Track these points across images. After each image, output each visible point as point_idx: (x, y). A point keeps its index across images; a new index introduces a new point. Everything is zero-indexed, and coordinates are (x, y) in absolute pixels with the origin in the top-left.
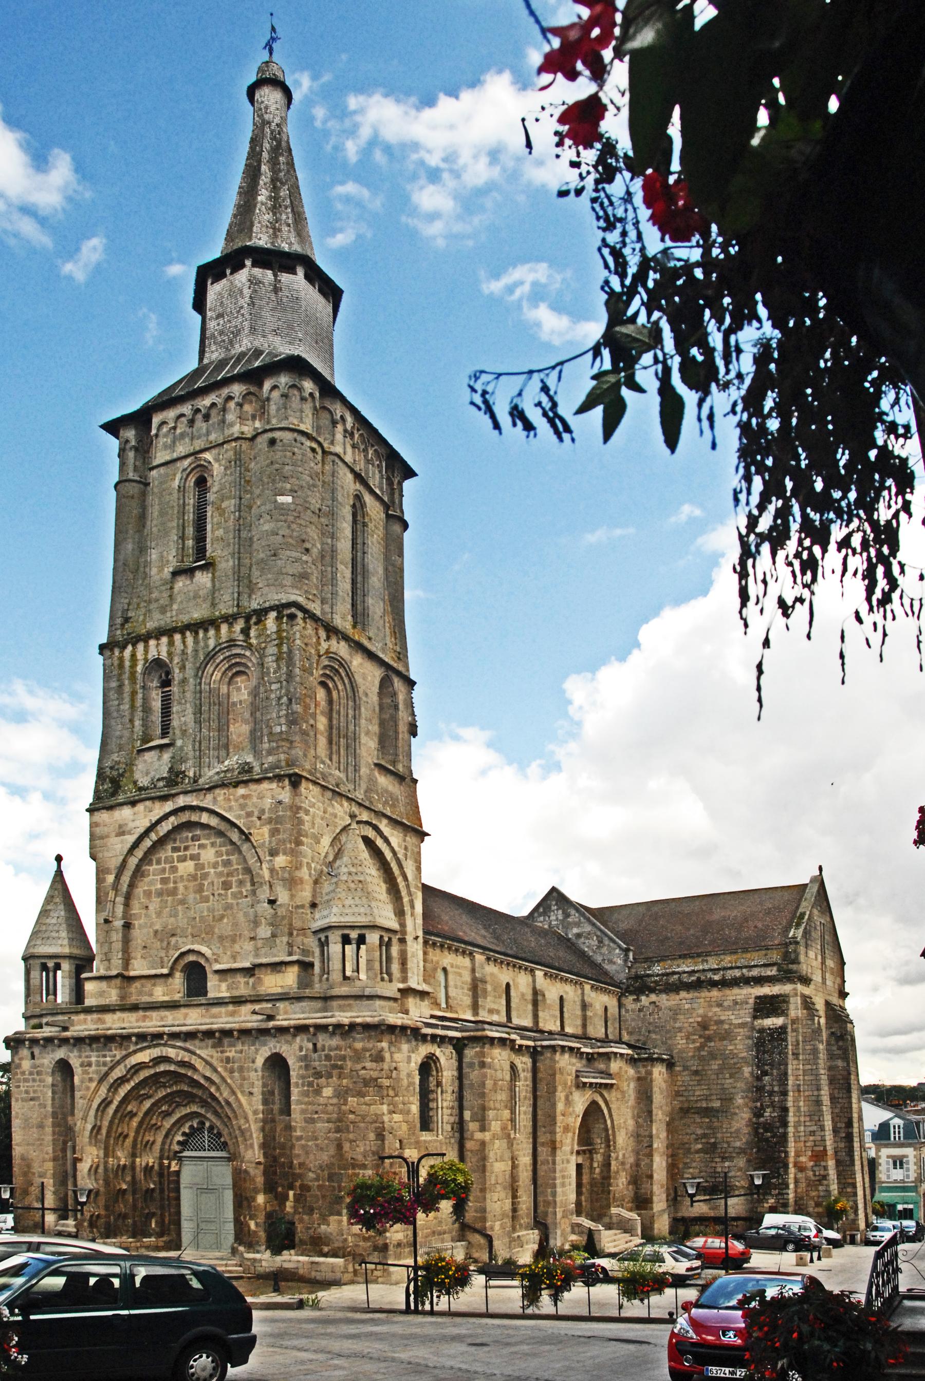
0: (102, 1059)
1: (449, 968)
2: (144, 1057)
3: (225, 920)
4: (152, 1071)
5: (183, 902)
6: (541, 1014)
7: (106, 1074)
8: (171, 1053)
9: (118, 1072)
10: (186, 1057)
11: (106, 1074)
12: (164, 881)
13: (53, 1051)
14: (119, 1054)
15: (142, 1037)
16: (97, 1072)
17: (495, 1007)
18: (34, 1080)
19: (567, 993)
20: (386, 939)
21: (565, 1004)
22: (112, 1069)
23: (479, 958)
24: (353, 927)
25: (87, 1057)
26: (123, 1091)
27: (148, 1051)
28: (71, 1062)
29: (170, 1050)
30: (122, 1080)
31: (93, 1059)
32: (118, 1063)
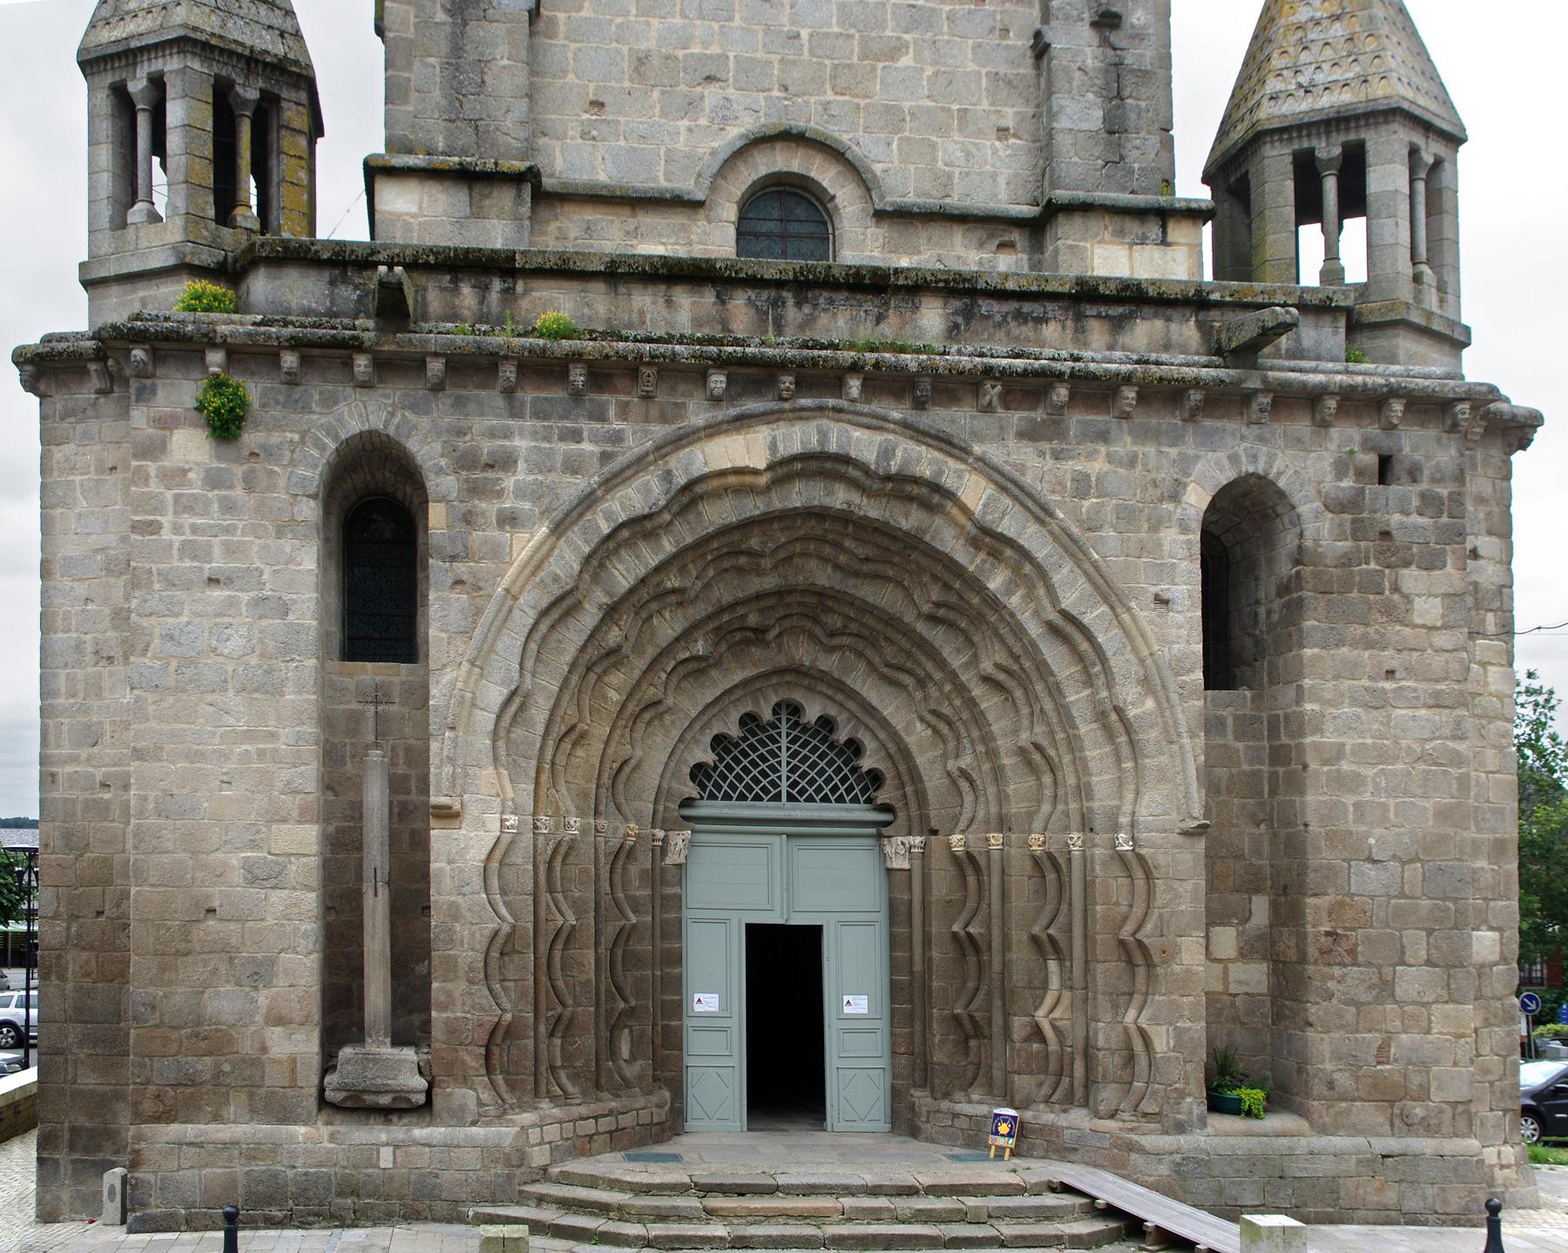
0: (563, 447)
2: (746, 449)
3: (906, 61)
4: (754, 507)
7: (588, 501)
8: (863, 444)
9: (632, 499)
10: (925, 461)
11: (588, 501)
13: (330, 401)
14: (636, 437)
22: (611, 482)
25: (492, 434)
26: (624, 573)
29: (857, 433)
30: (640, 527)
31: (521, 444)
32: (640, 463)
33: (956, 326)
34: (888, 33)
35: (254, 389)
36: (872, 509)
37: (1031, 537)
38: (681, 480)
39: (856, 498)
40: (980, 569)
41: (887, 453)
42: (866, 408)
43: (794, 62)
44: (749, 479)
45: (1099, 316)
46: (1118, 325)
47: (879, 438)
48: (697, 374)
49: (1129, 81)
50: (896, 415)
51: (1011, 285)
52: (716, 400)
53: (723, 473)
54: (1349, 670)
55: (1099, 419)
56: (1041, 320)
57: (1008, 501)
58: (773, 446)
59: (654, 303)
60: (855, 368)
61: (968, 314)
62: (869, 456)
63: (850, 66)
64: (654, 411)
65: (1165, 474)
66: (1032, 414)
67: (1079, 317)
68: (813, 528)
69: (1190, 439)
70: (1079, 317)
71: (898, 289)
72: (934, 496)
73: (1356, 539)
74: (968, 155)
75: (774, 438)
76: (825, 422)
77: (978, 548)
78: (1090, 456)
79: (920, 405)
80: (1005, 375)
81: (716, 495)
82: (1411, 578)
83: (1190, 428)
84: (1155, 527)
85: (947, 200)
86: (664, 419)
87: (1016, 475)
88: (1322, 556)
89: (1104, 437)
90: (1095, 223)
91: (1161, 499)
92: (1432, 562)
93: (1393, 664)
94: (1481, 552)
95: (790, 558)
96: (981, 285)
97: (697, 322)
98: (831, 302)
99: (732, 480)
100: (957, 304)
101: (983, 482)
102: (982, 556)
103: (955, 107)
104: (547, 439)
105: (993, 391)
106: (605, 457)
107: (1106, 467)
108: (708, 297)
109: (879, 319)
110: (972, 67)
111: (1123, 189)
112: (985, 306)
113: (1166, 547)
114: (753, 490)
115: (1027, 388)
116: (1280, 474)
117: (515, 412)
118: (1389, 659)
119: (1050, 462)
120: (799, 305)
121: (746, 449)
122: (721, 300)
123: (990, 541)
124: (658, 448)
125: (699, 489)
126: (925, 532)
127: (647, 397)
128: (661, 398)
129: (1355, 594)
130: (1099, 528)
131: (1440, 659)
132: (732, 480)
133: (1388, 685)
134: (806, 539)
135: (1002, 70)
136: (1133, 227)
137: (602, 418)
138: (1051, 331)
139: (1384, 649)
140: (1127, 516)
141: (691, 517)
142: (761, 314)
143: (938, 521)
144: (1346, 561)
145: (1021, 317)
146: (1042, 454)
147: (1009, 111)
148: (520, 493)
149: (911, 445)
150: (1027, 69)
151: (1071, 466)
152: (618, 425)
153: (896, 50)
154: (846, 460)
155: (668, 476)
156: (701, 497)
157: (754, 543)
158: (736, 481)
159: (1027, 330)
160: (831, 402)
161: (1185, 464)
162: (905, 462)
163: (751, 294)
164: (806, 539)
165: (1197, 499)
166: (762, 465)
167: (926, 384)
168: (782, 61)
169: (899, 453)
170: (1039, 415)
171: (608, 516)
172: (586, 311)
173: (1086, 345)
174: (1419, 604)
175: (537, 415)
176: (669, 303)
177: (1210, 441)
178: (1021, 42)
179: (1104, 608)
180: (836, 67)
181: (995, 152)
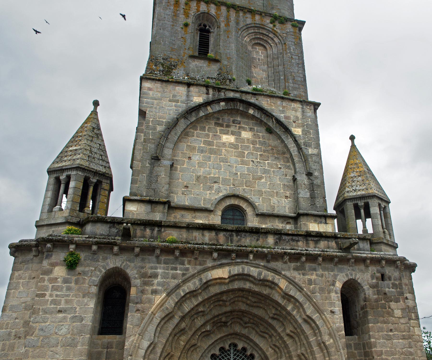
0: (172, 272)
2: (222, 273)
3: (263, 180)
4: (224, 288)
5: (225, 160)
8: (254, 271)
10: (270, 276)
11: (178, 287)
14: (192, 270)
15: (225, 254)
16: (161, 284)
18: (69, 289)
22: (185, 282)
25: (152, 268)
27: (227, 269)
28: (128, 271)
30: (193, 294)
32: (193, 276)
33: (277, 242)
34: (259, 174)
36: (256, 289)
37: (298, 296)
38: (204, 281)
39: (252, 286)
40: (285, 304)
41: (260, 274)
42: (254, 262)
43: (236, 180)
44: (223, 281)
45: (312, 240)
46: (316, 242)
47: (258, 270)
48: (210, 253)
49: (315, 187)
50: (262, 264)
51: (290, 232)
52: (214, 260)
53: (216, 279)
54: (381, 330)
55: (313, 265)
56: (298, 241)
57: (292, 286)
58: (230, 272)
59: (199, 235)
60: (251, 252)
61: (280, 239)
62: (255, 275)
63: (250, 181)
64: (198, 262)
65: (330, 279)
66: (297, 264)
67: (307, 240)
68: (240, 294)
69: (336, 270)
70: (307, 240)
71: (262, 233)
72: (273, 285)
73: (378, 295)
74: (278, 202)
75: (230, 270)
76: (244, 266)
77: (284, 299)
78: (312, 274)
79: (268, 261)
80: (289, 254)
81: (214, 285)
82: (393, 305)
83: (335, 267)
84: (329, 292)
85: (274, 212)
86: (200, 264)
87: (293, 279)
88: (371, 299)
89: (315, 270)
90: (309, 218)
91: (330, 285)
92: (397, 301)
93: (392, 328)
94: (408, 298)
95: (234, 302)
96: (283, 232)
97: (210, 240)
98: (245, 235)
99: (218, 281)
100: (277, 237)
101: (285, 281)
102: (285, 301)
103: (275, 191)
104: (168, 270)
105: (287, 258)
106: (184, 275)
107: (316, 277)
108: (213, 234)
109: (257, 240)
111: (315, 211)
112: (284, 237)
113: (332, 298)
114: (224, 284)
115: (296, 257)
116: (358, 279)
117: (159, 262)
118: (391, 326)
119: (302, 276)
120: (237, 236)
121: (222, 273)
122: (217, 234)
123: (287, 296)
124: (198, 272)
125: (209, 283)
126: (270, 294)
127: (196, 259)
128: (200, 259)
129: (380, 309)
130: (315, 293)
131: (402, 326)
132: (218, 281)
133: (391, 333)
134: (239, 297)
135: (286, 183)
136: (319, 219)
137: (183, 264)
138: (300, 243)
139: (389, 324)
140: (322, 290)
141: (207, 291)
142: (227, 238)
143: (274, 291)
144: (377, 301)
145: (293, 240)
146: (300, 274)
147: (288, 192)
148: (159, 284)
149: (266, 272)
150: (291, 183)
151: (307, 277)
152: (187, 266)
153: (261, 178)
154: (249, 275)
155: (201, 280)
156: (210, 286)
157: (224, 298)
158: (220, 281)
159: (294, 243)
160: (245, 261)
161: (335, 276)
162: (265, 276)
163: (225, 233)
164: (239, 297)
165: (339, 285)
166: (227, 277)
167: (270, 256)
168: (233, 179)
169: (263, 274)
170: (298, 264)
171: (183, 291)
172: (180, 236)
173: (309, 247)
174: (396, 311)
175: (165, 263)
176: (203, 235)
177: (341, 271)
178: (290, 178)
179: (318, 314)
180: (246, 181)
181: (285, 201)
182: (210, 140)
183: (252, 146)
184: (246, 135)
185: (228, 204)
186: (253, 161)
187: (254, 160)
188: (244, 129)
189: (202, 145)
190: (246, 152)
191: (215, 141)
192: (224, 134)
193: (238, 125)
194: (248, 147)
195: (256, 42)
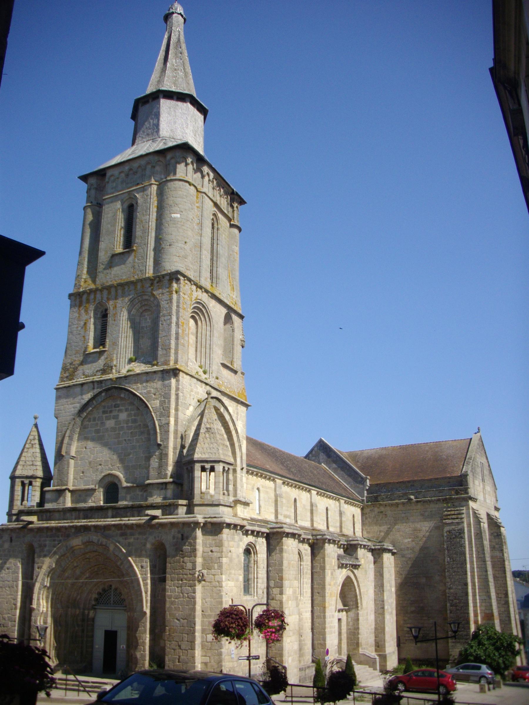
1: (261, 489)
3: (131, 456)
6: (315, 519)
10: (104, 541)
12: (97, 431)
17: (288, 513)
19: (330, 505)
20: (226, 469)
21: (329, 512)
23: (279, 482)
24: (207, 462)
31: (47, 542)
35: (14, 535)
62: (96, 541)
108: (77, 513)
110: (142, 455)
137: (58, 537)
152: (61, 538)
153: (129, 455)
182: (98, 428)
183: (125, 425)
184: (123, 416)
185: (107, 481)
186: (125, 440)
187: (126, 438)
188: (120, 411)
189: (94, 434)
190: (121, 433)
191: (101, 429)
192: (108, 420)
193: (118, 408)
194: (123, 427)
195: (144, 309)
